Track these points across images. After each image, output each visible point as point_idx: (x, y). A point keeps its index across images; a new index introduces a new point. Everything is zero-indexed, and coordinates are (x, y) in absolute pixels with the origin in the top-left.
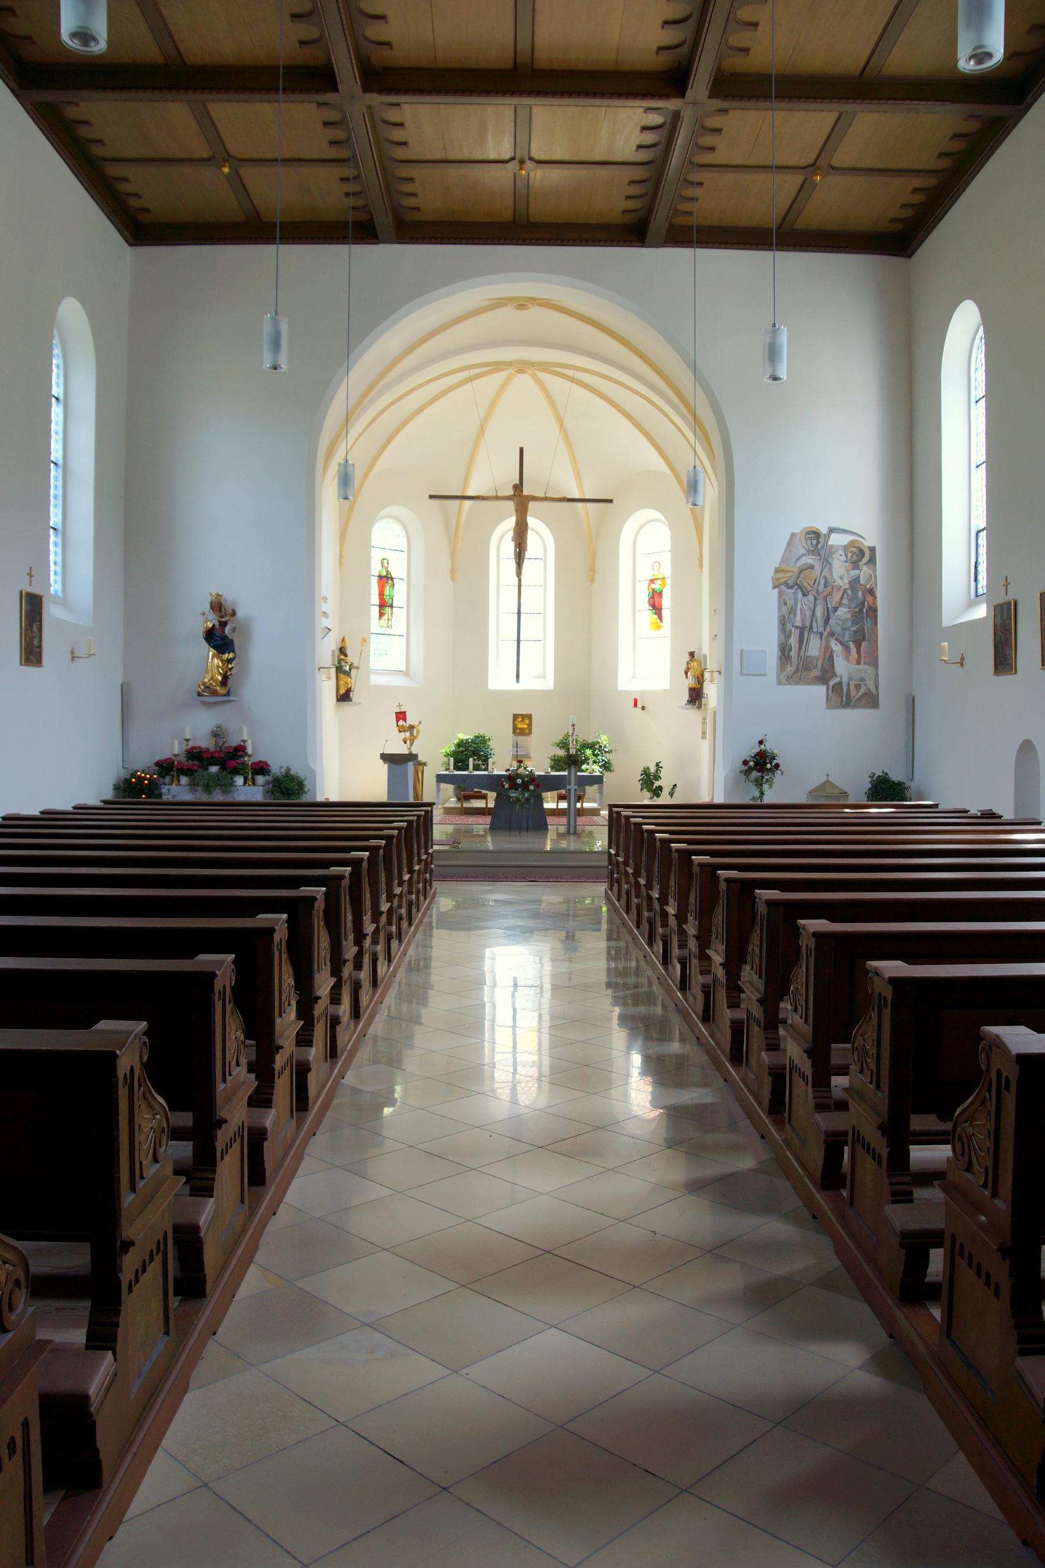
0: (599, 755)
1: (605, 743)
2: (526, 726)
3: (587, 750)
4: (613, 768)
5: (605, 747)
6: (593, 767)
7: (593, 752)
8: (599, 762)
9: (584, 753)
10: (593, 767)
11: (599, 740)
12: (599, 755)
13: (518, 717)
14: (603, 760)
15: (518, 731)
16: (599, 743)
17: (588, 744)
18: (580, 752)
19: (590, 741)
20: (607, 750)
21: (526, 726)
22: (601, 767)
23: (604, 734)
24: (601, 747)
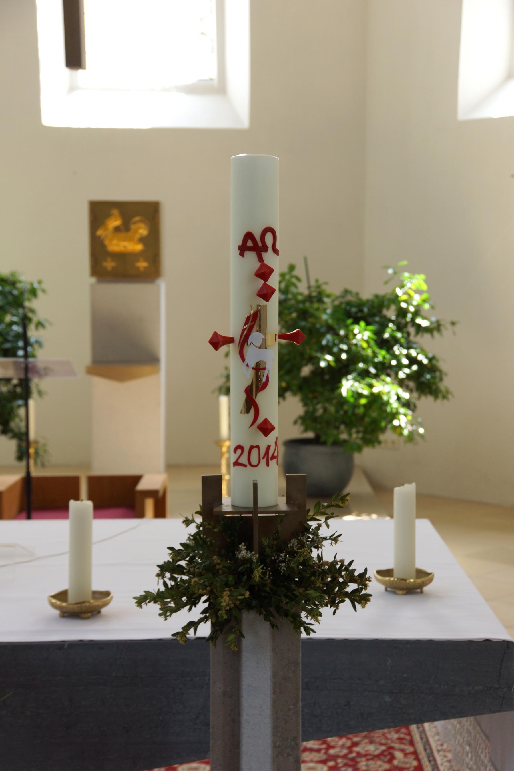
0: (395, 341)
1: (417, 299)
2: (139, 247)
3: (356, 329)
4: (445, 384)
5: (417, 313)
6: (378, 387)
7: (379, 333)
8: (400, 366)
9: (345, 339)
10: (378, 387)
11: (399, 292)
12: (395, 341)
13: (108, 215)
14: (413, 361)
15: (109, 265)
16: (395, 299)
17: (360, 305)
18: (336, 334)
19: (366, 295)
20: (424, 323)
21: (139, 247)
22: (401, 383)
23: (414, 271)
24: (403, 312)
